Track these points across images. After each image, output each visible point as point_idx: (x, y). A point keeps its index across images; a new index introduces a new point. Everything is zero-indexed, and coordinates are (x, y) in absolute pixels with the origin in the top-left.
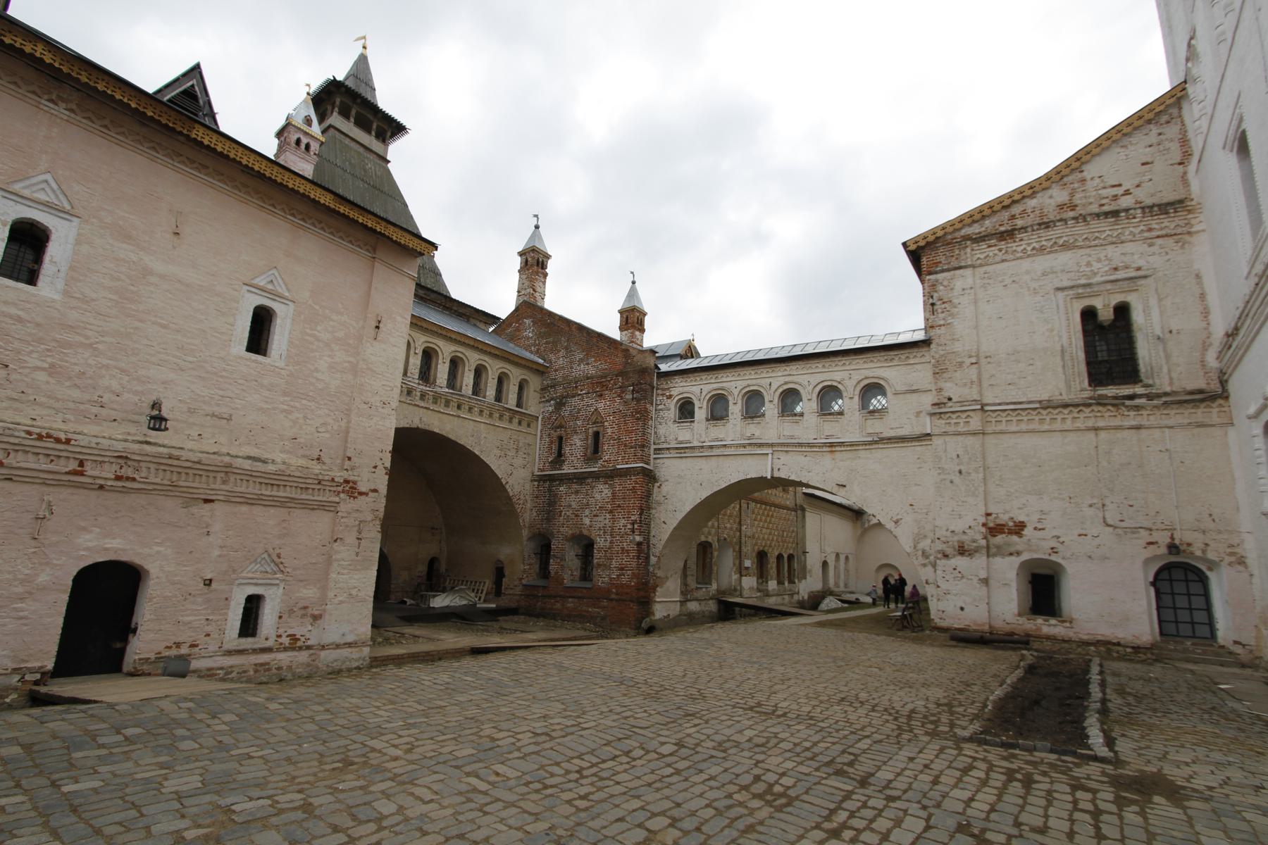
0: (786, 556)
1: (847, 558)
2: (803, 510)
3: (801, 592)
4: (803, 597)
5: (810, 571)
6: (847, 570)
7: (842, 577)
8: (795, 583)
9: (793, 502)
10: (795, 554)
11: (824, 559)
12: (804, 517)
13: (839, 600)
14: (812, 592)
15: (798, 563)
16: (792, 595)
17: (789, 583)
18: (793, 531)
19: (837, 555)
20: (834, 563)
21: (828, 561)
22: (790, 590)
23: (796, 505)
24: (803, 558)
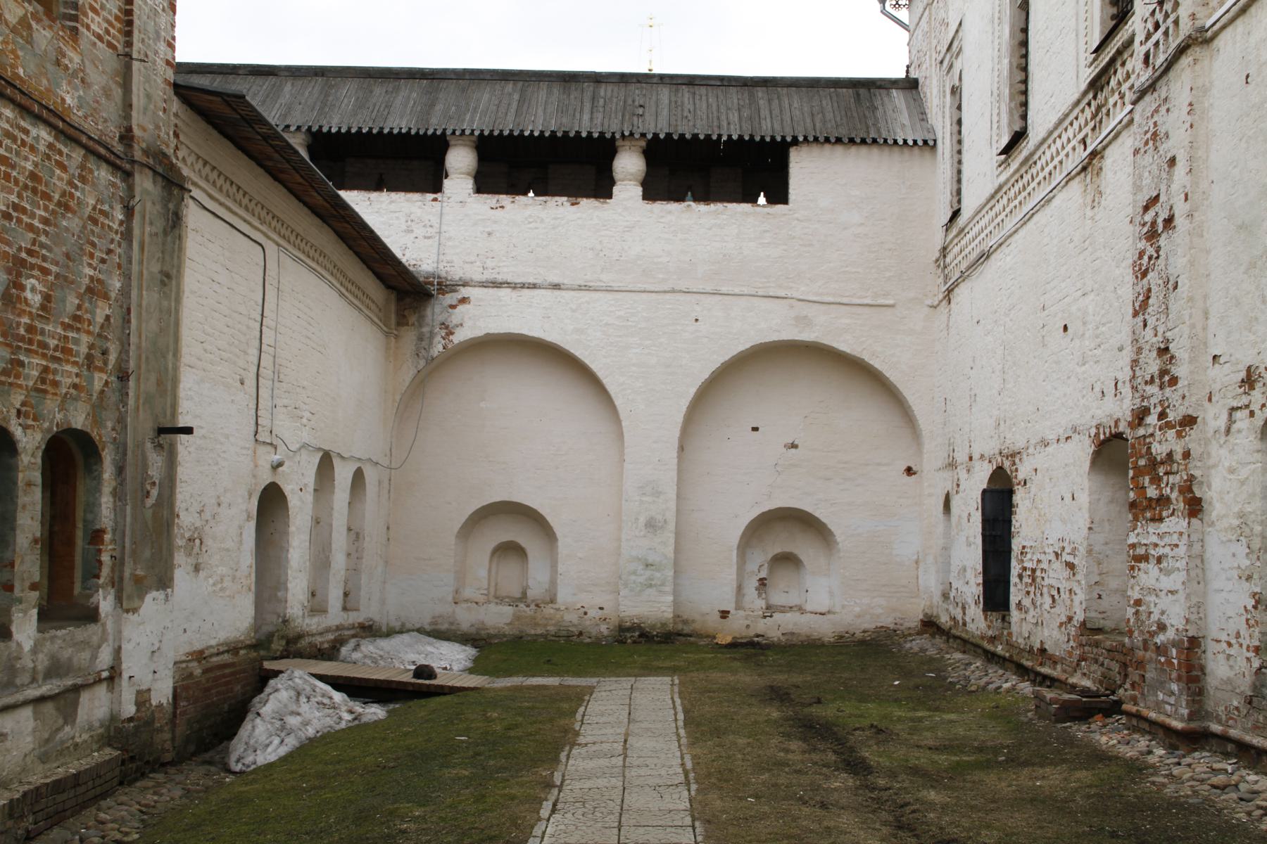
0: (30, 443)
1: (358, 476)
2: (173, 184)
3: (131, 666)
4: (142, 699)
5: (195, 541)
6: (355, 534)
7: (339, 560)
8: (92, 616)
9: (110, 110)
10: (104, 434)
11: (266, 478)
12: (175, 222)
13: (338, 683)
14: (199, 656)
15: (117, 494)
16: (67, 700)
17: (47, 617)
18: (96, 291)
19: (326, 463)
20: (309, 497)
21: (287, 489)
22: (56, 669)
23: (127, 137)
24: (156, 463)
